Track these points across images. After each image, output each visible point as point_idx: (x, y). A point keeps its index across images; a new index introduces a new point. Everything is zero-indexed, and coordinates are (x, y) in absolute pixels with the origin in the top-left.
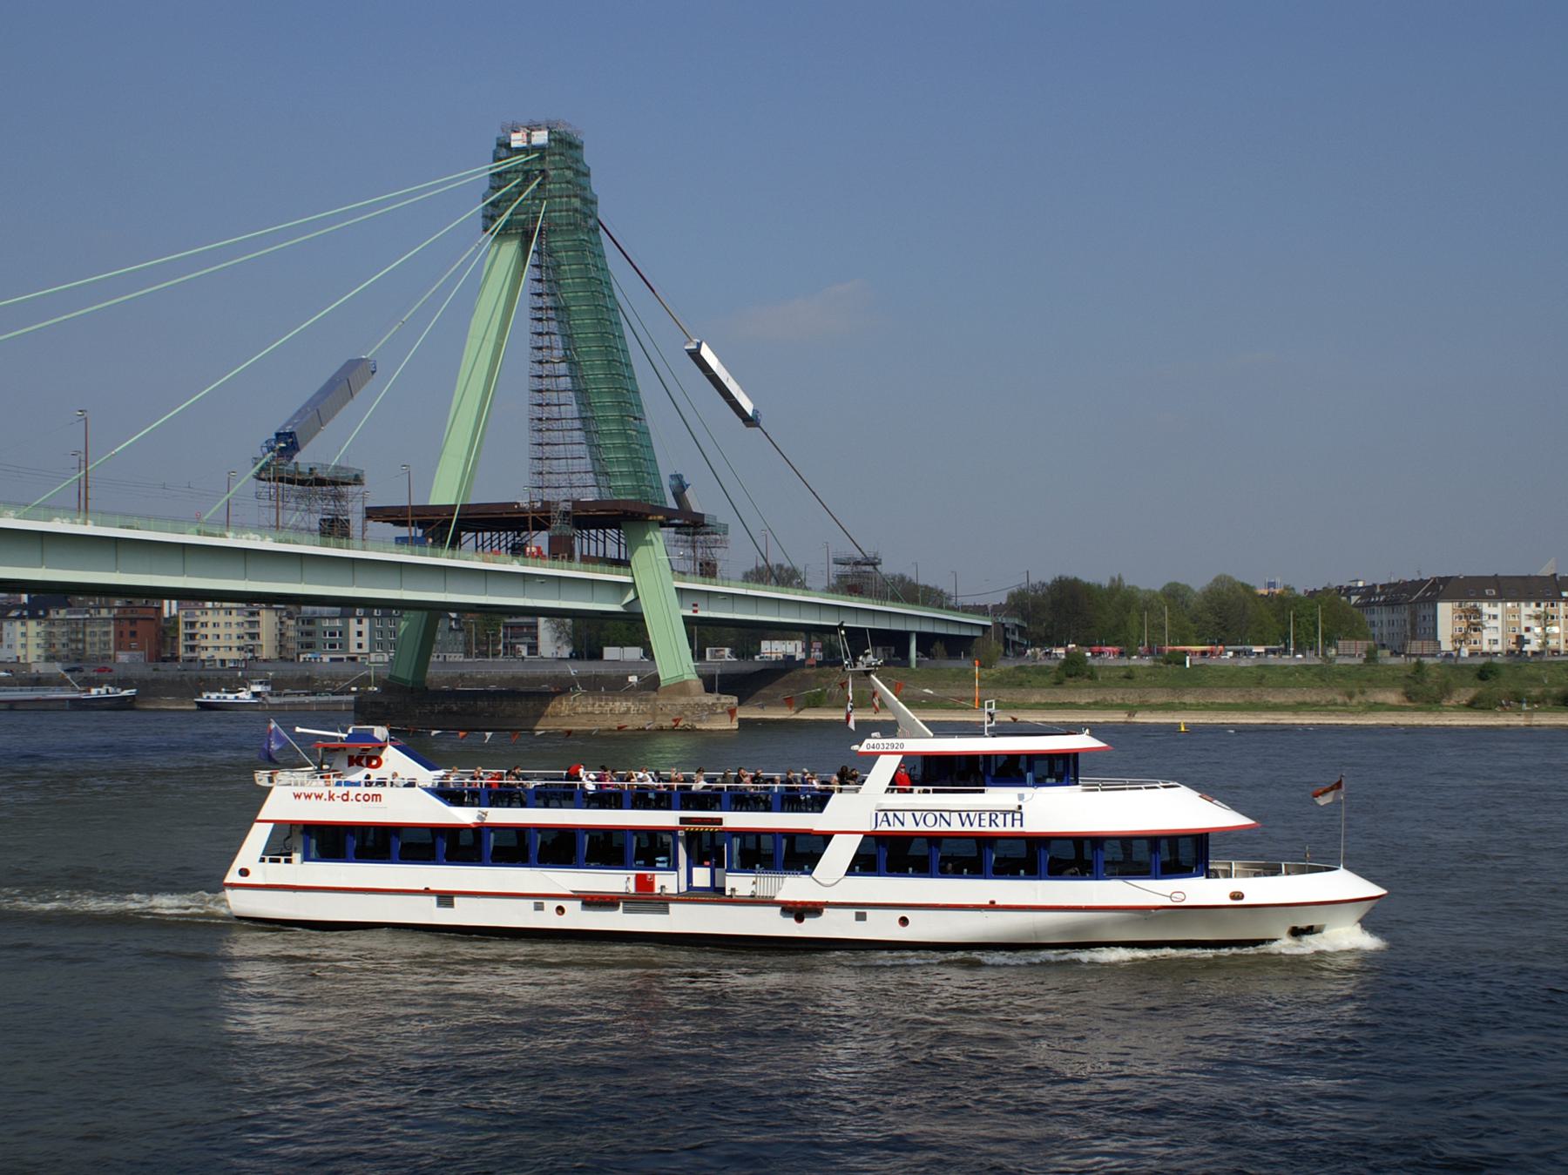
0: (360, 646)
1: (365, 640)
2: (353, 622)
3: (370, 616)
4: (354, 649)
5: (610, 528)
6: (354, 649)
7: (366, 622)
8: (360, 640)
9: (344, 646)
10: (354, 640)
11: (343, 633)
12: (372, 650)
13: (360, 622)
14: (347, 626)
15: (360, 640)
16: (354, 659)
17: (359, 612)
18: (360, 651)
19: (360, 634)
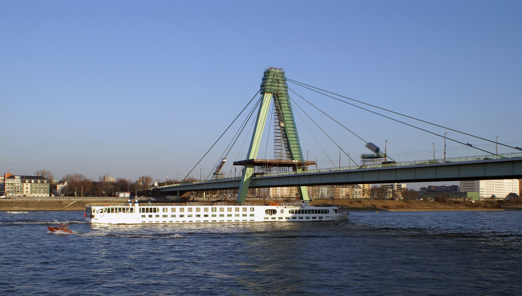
0: (27, 192)
1: (29, 190)
2: (25, 184)
3: (30, 182)
4: (25, 193)
5: (290, 167)
6: (25, 193)
7: (29, 184)
8: (27, 190)
9: (22, 192)
10: (25, 190)
11: (22, 188)
12: (31, 193)
13: (27, 185)
14: (23, 186)
15: (27, 190)
16: (25, 196)
17: (27, 181)
18: (27, 193)
19: (27, 188)
